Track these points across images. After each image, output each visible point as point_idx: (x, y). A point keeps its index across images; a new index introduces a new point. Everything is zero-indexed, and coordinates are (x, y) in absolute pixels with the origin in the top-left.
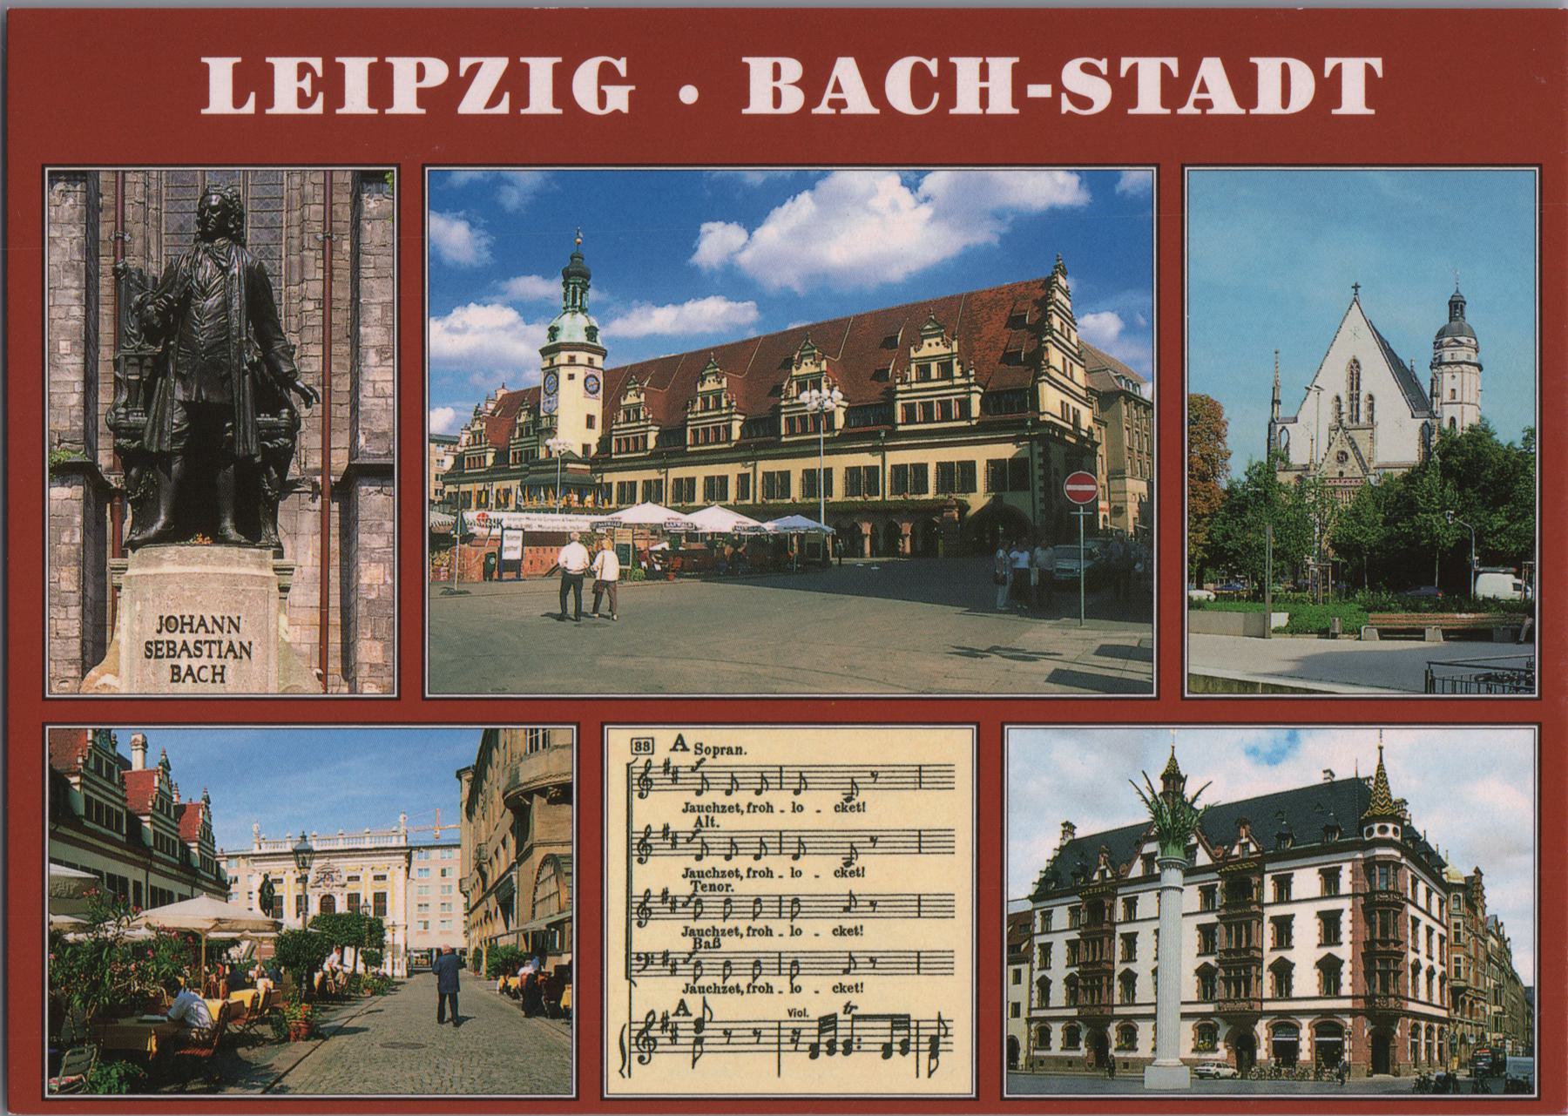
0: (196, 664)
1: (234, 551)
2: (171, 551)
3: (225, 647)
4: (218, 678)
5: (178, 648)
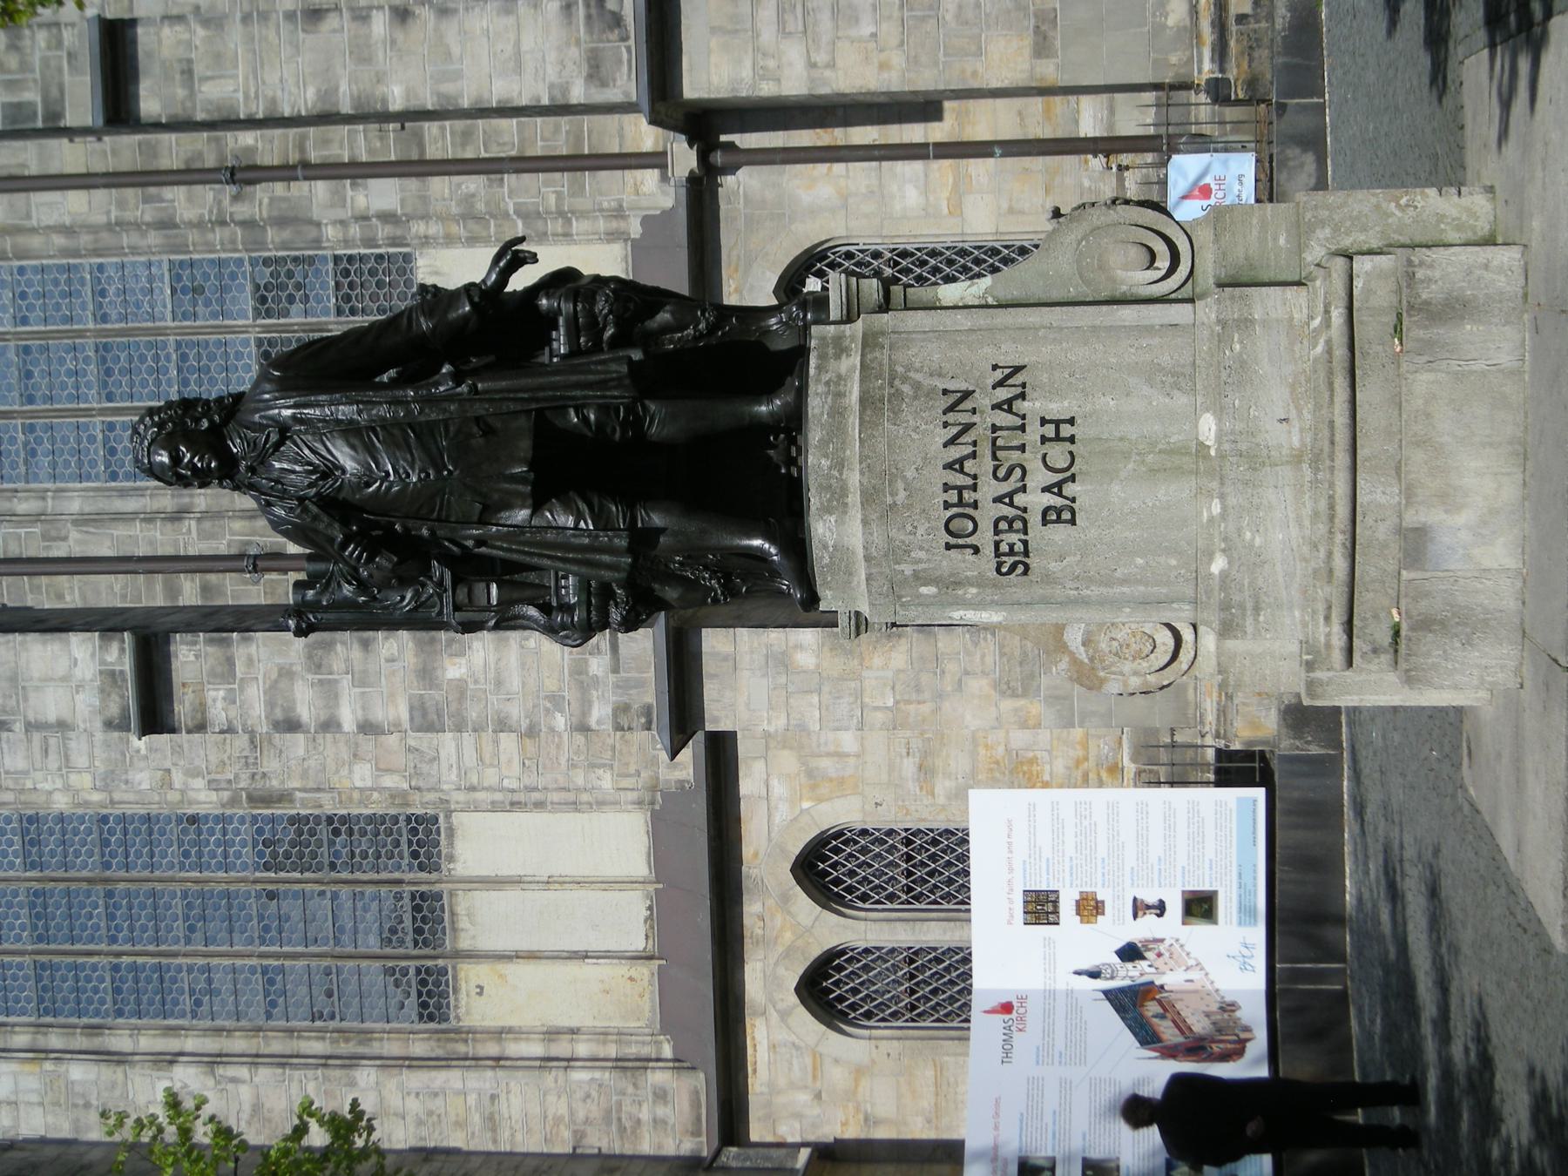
0: (1039, 477)
1: (816, 405)
2: (822, 529)
4: (1066, 430)
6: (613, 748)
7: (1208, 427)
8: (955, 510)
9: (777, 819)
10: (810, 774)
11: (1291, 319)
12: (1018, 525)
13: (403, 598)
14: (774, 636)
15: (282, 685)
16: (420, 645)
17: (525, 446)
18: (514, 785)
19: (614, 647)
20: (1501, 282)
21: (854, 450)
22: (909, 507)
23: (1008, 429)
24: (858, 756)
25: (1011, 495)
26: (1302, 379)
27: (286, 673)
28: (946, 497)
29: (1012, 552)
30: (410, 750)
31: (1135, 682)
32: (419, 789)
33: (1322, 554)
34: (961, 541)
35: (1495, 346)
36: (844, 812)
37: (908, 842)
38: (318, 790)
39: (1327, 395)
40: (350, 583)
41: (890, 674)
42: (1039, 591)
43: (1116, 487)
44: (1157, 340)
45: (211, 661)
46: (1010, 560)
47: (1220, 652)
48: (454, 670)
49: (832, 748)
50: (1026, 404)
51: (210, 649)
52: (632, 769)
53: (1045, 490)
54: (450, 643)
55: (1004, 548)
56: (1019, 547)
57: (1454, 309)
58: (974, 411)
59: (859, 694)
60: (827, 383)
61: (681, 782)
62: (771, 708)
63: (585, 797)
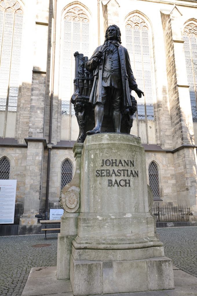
2: (106, 135)
3: (129, 172)
4: (128, 185)
5: (111, 172)
6: (24, 134)
7: (129, 215)
8: (111, 162)
9: (12, 155)
10: (19, 159)
11: (148, 233)
12: (108, 175)
13: (81, 71)
14: (41, 154)
15: (38, 90)
16: (43, 108)
17: (116, 87)
18: (20, 120)
19: (40, 133)
20: (167, 283)
21: (121, 142)
22: (112, 152)
23: (128, 173)
24: (21, 166)
25: (115, 173)
26: (140, 236)
27: (40, 90)
28: (114, 160)
29: (102, 173)
30: (26, 108)
31: (64, 200)
32: (21, 108)
33: (104, 242)
34: (104, 163)
35: (153, 284)
36: (12, 163)
37: (7, 172)
38: (21, 96)
39: (138, 242)
40: (84, 63)
41: (34, 169)
42: (92, 179)
43: (116, 195)
44: (143, 204)
45: (42, 81)
46: (100, 172)
47: (69, 218)
48: (39, 112)
49: (22, 162)
50: (132, 177)
51: (43, 81)
52: (21, 136)
53: (116, 181)
54: (43, 112)
55: (103, 172)
56: (103, 175)
57: (160, 271)
58: (130, 166)
59: (32, 165)
60: (133, 139)
61: (19, 142)
62: (31, 153)
63: (17, 130)
